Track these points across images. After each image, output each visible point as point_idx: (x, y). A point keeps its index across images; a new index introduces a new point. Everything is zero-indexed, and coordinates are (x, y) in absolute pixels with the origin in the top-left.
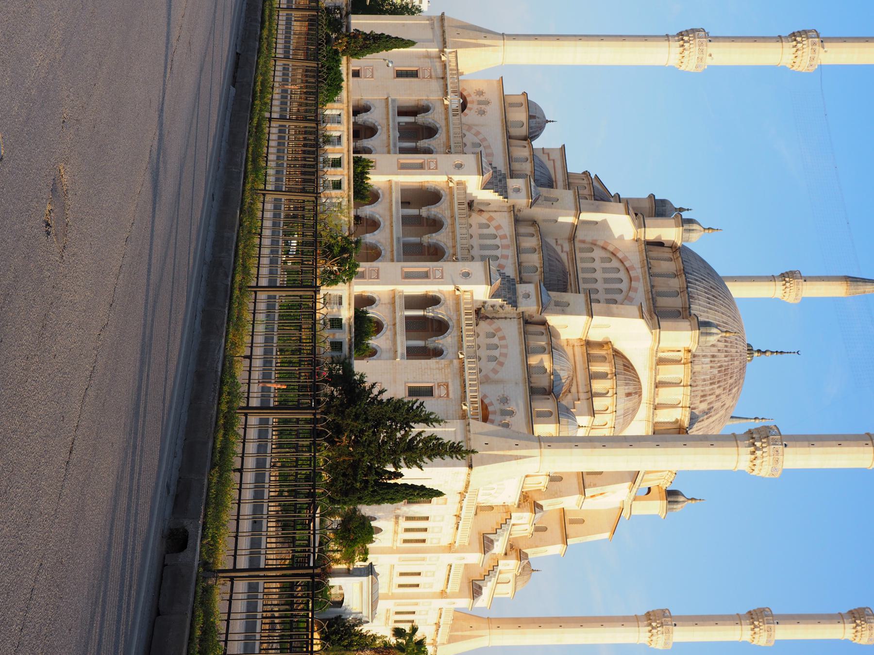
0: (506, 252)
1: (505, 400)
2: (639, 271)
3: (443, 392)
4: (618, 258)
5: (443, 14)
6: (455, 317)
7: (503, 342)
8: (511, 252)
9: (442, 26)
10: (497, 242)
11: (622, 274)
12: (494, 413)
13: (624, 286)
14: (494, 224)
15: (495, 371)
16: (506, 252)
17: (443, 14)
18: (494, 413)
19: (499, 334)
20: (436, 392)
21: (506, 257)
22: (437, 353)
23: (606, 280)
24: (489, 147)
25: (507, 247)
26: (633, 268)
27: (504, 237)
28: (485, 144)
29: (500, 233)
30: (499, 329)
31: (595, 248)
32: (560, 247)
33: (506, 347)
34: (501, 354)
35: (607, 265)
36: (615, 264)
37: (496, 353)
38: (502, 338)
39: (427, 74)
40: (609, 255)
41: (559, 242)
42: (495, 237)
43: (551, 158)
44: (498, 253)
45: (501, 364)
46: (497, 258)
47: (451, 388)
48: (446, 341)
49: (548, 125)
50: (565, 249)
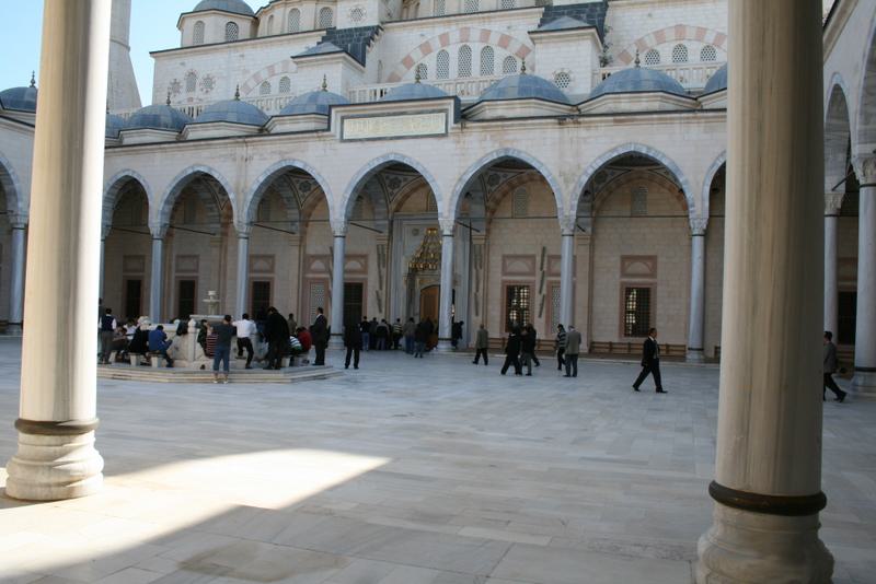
0: (475, 34)
8: (476, 27)
10: (453, 52)
14: (417, 57)
16: (475, 34)
19: (651, 42)
21: (486, 34)
24: (271, 69)
25: (465, 33)
27: (444, 39)
28: (264, 75)
29: (437, 46)
34: (699, 38)
42: (443, 56)
44: (476, 48)
46: (487, 51)
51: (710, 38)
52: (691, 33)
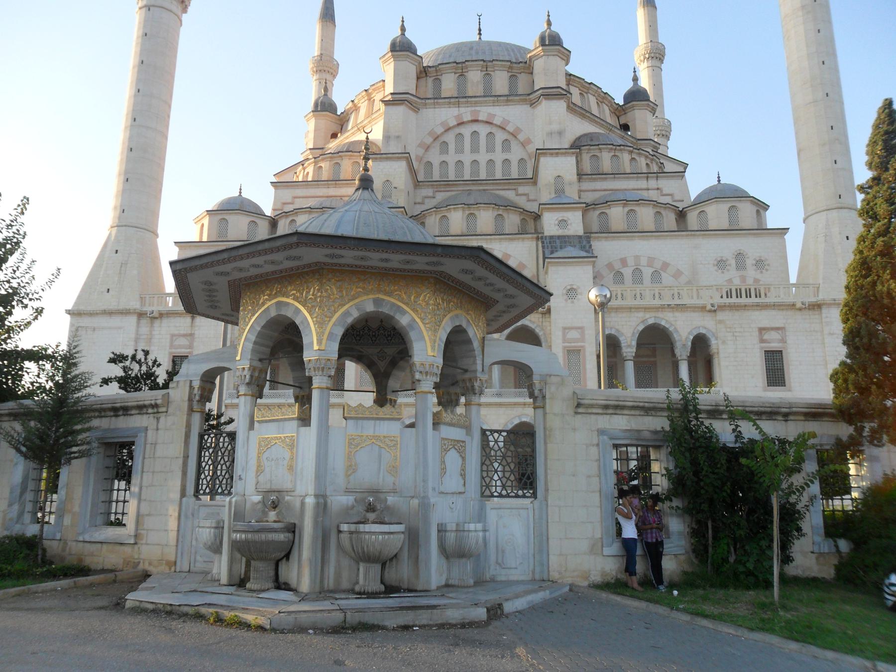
1: (721, 264)
2: (462, 110)
3: (774, 335)
4: (442, 133)
5: (68, 312)
6: (641, 315)
7: (631, 262)
9: (91, 314)
11: (467, 131)
12: (743, 279)
13: (483, 130)
15: (678, 274)
17: (68, 312)
18: (743, 279)
19: (617, 266)
20: (775, 346)
22: (700, 344)
23: (475, 149)
26: (458, 117)
30: (610, 266)
31: (425, 160)
32: (427, 200)
33: (637, 258)
34: (650, 265)
35: (452, 147)
36: (450, 138)
37: (647, 272)
38: (624, 262)
39: (183, 341)
40: (437, 144)
41: (419, 200)
43: (289, 200)
45: (665, 266)
47: (765, 324)
48: (683, 329)
49: (244, 195)
50: (431, 194)
51: (658, 265)
52: (644, 261)
